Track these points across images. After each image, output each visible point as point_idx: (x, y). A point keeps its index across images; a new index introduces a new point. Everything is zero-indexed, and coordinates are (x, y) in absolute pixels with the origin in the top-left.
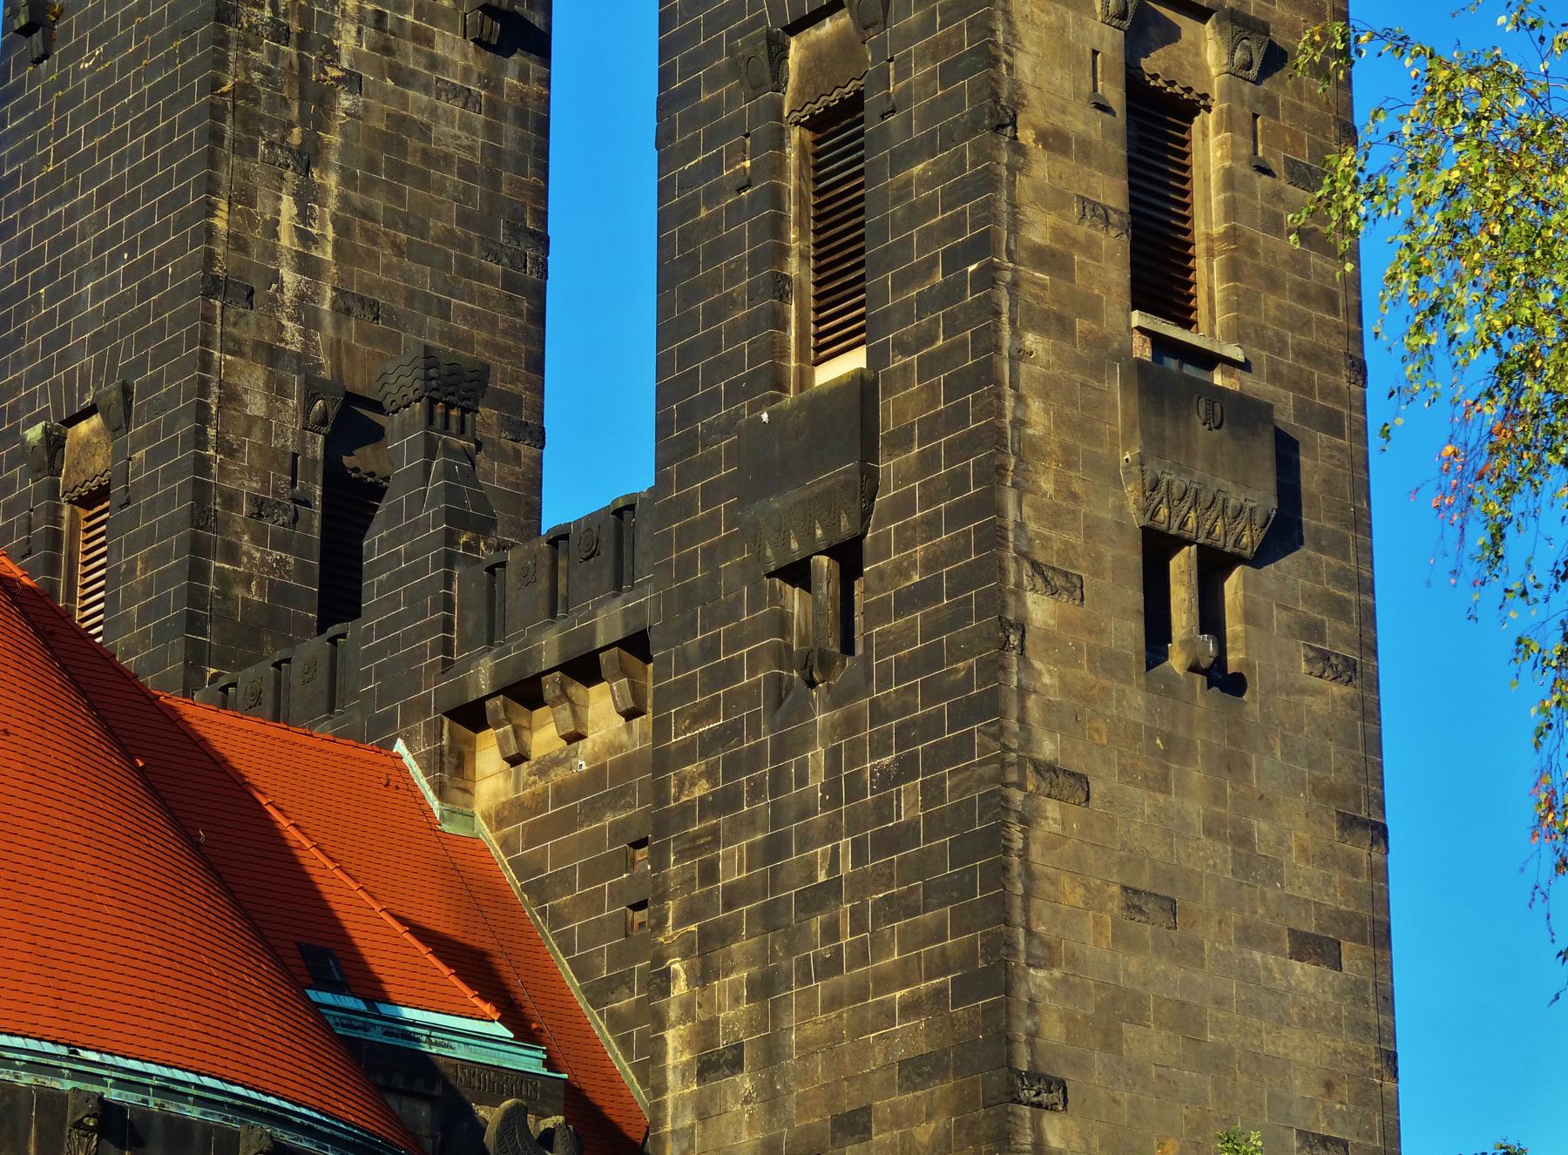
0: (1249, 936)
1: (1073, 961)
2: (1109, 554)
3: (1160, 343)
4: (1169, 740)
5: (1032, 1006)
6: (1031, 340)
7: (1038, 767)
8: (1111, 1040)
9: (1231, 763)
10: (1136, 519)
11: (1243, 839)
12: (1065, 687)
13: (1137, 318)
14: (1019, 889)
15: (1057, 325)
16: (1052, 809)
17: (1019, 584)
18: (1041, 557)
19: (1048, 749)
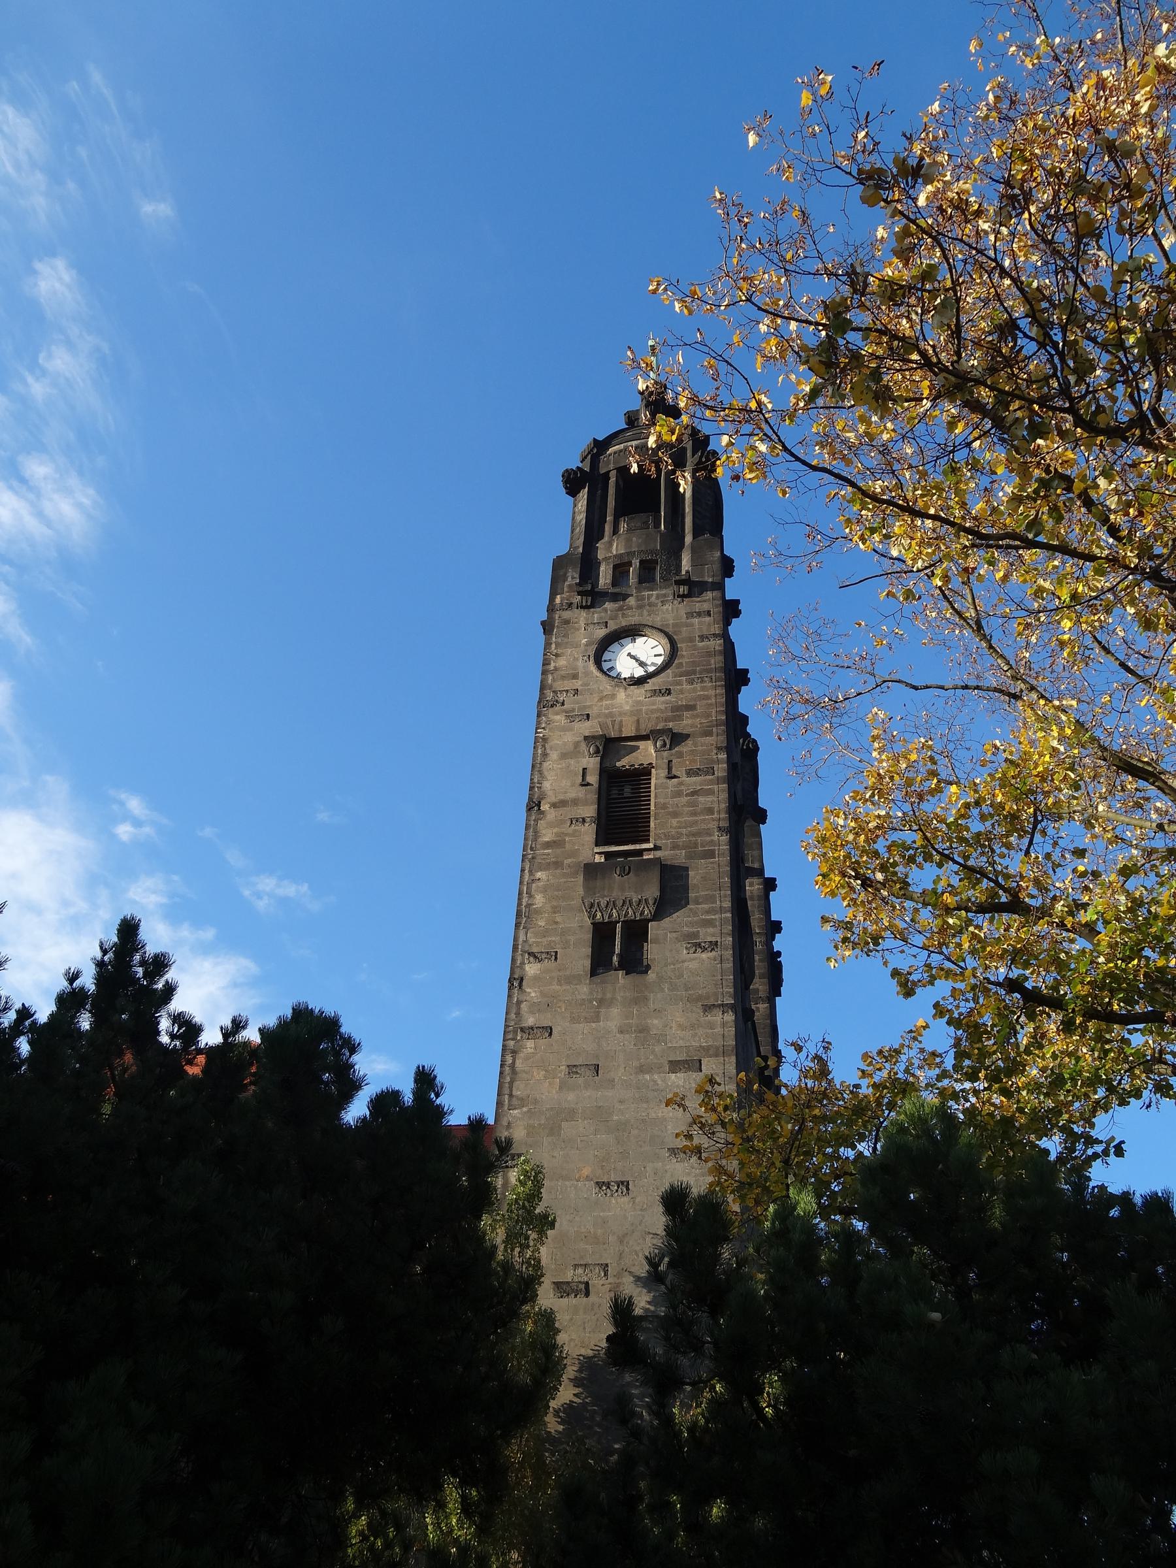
0: (642, 1070)
1: (536, 1102)
2: (572, 938)
3: (608, 855)
4: (601, 1002)
5: (509, 1126)
6: (539, 875)
7: (522, 1029)
8: (554, 1130)
9: (640, 1000)
10: (588, 922)
11: (643, 1030)
12: (543, 994)
13: (597, 850)
14: (508, 1079)
15: (557, 865)
16: (530, 1044)
17: (523, 963)
18: (535, 950)
19: (530, 1021)
